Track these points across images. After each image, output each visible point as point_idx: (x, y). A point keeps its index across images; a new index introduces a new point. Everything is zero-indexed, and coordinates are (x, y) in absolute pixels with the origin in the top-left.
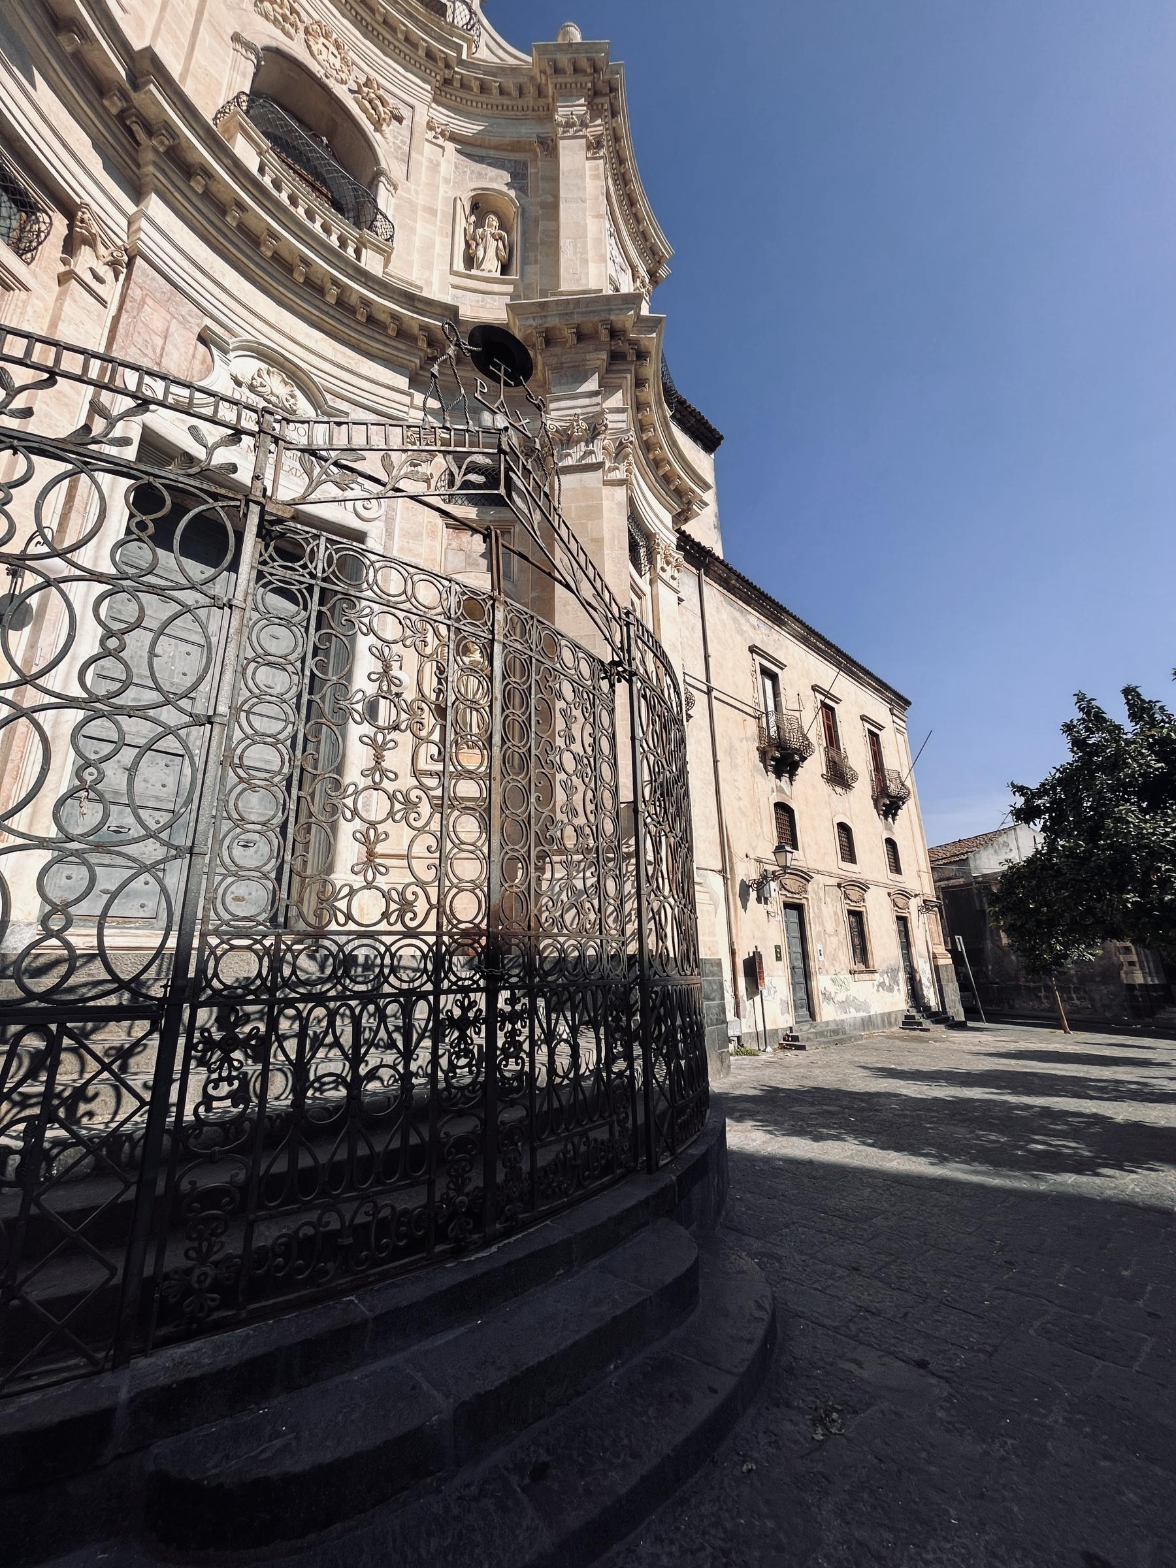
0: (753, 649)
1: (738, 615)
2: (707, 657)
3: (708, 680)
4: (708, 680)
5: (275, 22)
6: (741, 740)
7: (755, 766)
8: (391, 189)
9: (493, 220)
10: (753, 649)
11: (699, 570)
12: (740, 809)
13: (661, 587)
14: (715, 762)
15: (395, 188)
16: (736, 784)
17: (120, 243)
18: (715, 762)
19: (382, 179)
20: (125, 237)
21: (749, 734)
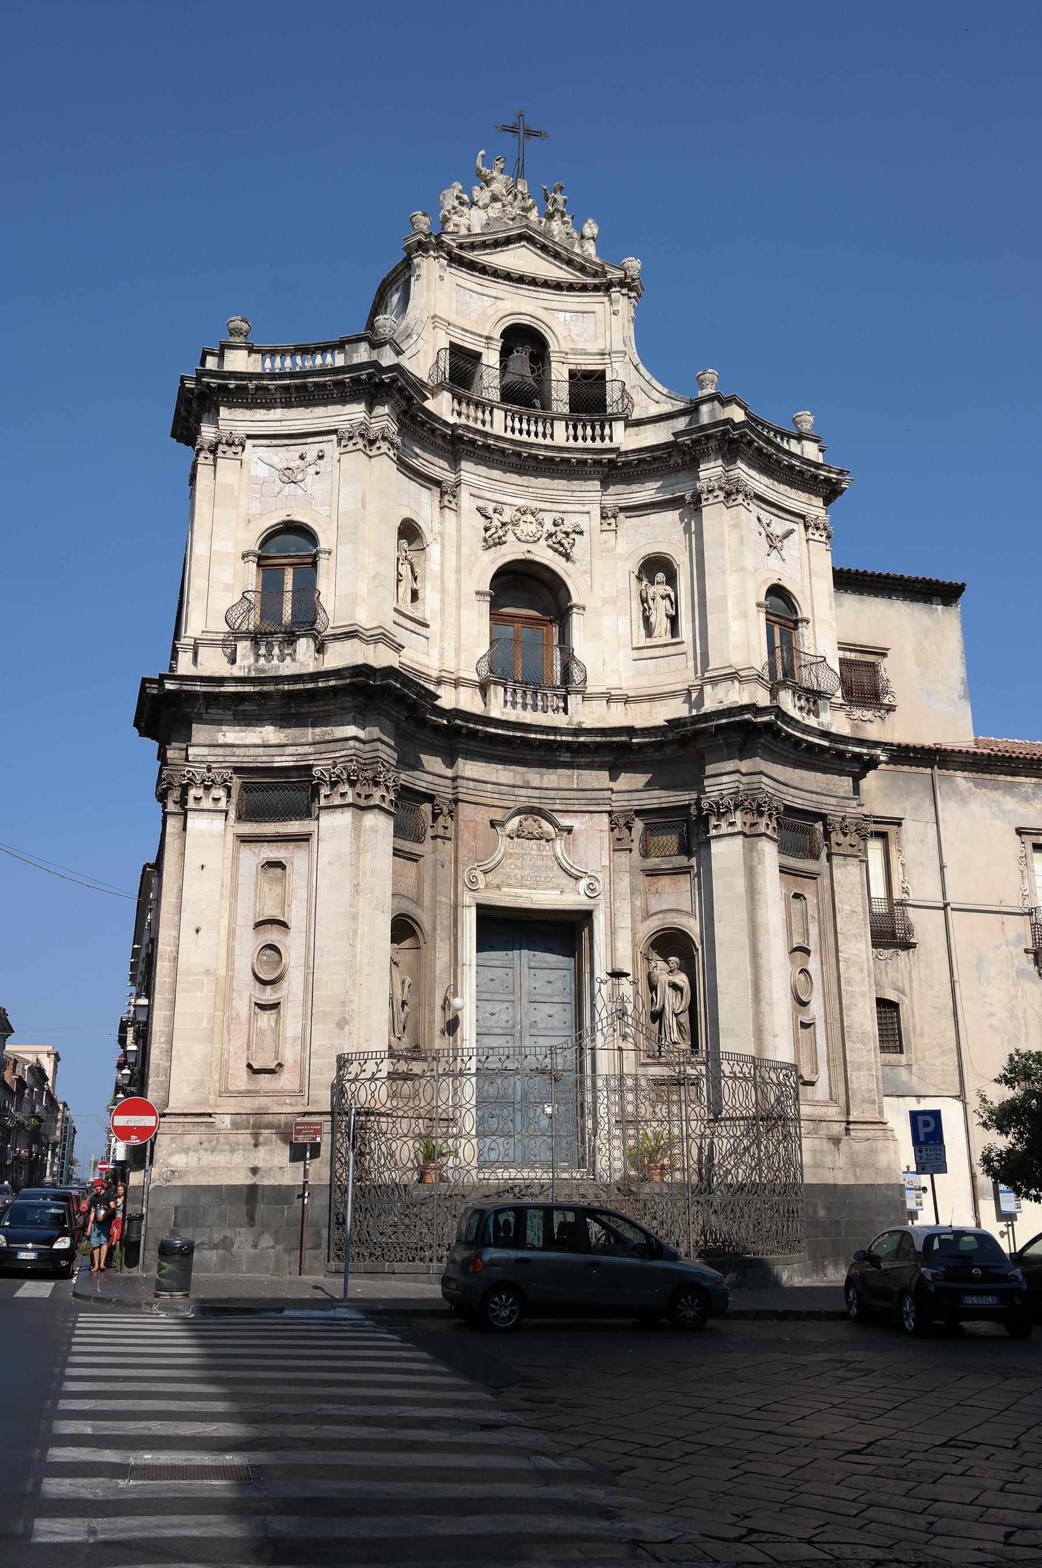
0: (1020, 832)
1: (997, 795)
2: (942, 868)
3: (944, 894)
4: (944, 894)
5: (495, 545)
6: (998, 947)
7: (1021, 973)
8: (581, 611)
9: (660, 576)
10: (1020, 832)
11: (932, 768)
12: (991, 1026)
13: (835, 860)
14: (953, 983)
15: (584, 609)
16: (987, 999)
17: (451, 797)
18: (953, 983)
19: (575, 610)
20: (449, 790)
21: (1011, 936)
